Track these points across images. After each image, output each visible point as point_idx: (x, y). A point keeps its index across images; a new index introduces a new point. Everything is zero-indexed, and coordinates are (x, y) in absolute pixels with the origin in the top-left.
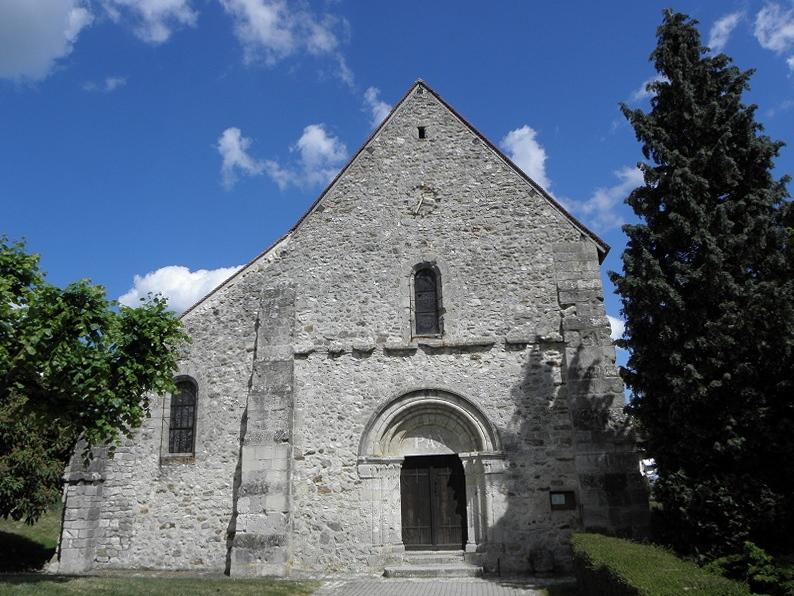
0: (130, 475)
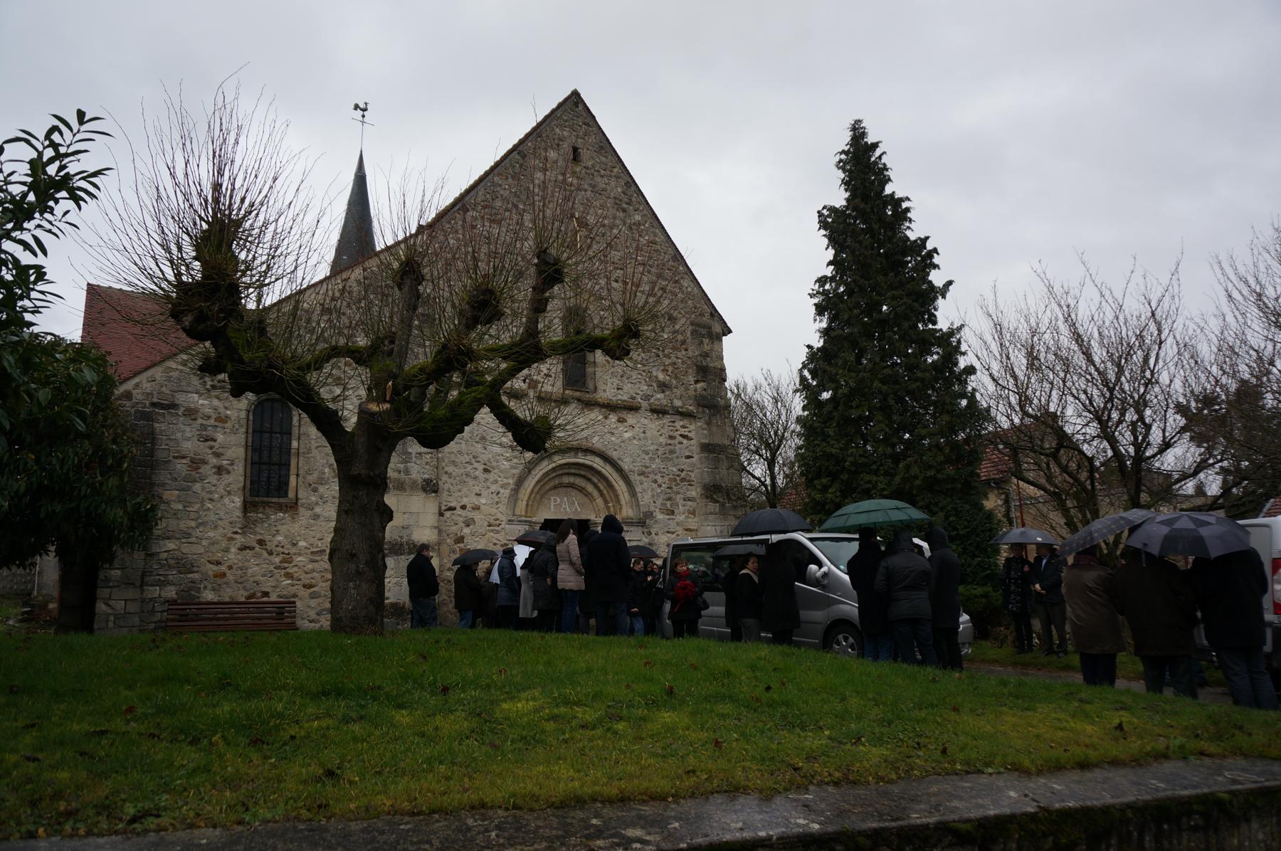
0: (193, 524)
